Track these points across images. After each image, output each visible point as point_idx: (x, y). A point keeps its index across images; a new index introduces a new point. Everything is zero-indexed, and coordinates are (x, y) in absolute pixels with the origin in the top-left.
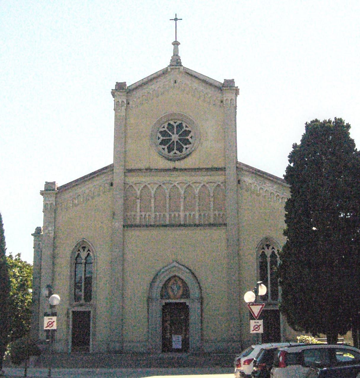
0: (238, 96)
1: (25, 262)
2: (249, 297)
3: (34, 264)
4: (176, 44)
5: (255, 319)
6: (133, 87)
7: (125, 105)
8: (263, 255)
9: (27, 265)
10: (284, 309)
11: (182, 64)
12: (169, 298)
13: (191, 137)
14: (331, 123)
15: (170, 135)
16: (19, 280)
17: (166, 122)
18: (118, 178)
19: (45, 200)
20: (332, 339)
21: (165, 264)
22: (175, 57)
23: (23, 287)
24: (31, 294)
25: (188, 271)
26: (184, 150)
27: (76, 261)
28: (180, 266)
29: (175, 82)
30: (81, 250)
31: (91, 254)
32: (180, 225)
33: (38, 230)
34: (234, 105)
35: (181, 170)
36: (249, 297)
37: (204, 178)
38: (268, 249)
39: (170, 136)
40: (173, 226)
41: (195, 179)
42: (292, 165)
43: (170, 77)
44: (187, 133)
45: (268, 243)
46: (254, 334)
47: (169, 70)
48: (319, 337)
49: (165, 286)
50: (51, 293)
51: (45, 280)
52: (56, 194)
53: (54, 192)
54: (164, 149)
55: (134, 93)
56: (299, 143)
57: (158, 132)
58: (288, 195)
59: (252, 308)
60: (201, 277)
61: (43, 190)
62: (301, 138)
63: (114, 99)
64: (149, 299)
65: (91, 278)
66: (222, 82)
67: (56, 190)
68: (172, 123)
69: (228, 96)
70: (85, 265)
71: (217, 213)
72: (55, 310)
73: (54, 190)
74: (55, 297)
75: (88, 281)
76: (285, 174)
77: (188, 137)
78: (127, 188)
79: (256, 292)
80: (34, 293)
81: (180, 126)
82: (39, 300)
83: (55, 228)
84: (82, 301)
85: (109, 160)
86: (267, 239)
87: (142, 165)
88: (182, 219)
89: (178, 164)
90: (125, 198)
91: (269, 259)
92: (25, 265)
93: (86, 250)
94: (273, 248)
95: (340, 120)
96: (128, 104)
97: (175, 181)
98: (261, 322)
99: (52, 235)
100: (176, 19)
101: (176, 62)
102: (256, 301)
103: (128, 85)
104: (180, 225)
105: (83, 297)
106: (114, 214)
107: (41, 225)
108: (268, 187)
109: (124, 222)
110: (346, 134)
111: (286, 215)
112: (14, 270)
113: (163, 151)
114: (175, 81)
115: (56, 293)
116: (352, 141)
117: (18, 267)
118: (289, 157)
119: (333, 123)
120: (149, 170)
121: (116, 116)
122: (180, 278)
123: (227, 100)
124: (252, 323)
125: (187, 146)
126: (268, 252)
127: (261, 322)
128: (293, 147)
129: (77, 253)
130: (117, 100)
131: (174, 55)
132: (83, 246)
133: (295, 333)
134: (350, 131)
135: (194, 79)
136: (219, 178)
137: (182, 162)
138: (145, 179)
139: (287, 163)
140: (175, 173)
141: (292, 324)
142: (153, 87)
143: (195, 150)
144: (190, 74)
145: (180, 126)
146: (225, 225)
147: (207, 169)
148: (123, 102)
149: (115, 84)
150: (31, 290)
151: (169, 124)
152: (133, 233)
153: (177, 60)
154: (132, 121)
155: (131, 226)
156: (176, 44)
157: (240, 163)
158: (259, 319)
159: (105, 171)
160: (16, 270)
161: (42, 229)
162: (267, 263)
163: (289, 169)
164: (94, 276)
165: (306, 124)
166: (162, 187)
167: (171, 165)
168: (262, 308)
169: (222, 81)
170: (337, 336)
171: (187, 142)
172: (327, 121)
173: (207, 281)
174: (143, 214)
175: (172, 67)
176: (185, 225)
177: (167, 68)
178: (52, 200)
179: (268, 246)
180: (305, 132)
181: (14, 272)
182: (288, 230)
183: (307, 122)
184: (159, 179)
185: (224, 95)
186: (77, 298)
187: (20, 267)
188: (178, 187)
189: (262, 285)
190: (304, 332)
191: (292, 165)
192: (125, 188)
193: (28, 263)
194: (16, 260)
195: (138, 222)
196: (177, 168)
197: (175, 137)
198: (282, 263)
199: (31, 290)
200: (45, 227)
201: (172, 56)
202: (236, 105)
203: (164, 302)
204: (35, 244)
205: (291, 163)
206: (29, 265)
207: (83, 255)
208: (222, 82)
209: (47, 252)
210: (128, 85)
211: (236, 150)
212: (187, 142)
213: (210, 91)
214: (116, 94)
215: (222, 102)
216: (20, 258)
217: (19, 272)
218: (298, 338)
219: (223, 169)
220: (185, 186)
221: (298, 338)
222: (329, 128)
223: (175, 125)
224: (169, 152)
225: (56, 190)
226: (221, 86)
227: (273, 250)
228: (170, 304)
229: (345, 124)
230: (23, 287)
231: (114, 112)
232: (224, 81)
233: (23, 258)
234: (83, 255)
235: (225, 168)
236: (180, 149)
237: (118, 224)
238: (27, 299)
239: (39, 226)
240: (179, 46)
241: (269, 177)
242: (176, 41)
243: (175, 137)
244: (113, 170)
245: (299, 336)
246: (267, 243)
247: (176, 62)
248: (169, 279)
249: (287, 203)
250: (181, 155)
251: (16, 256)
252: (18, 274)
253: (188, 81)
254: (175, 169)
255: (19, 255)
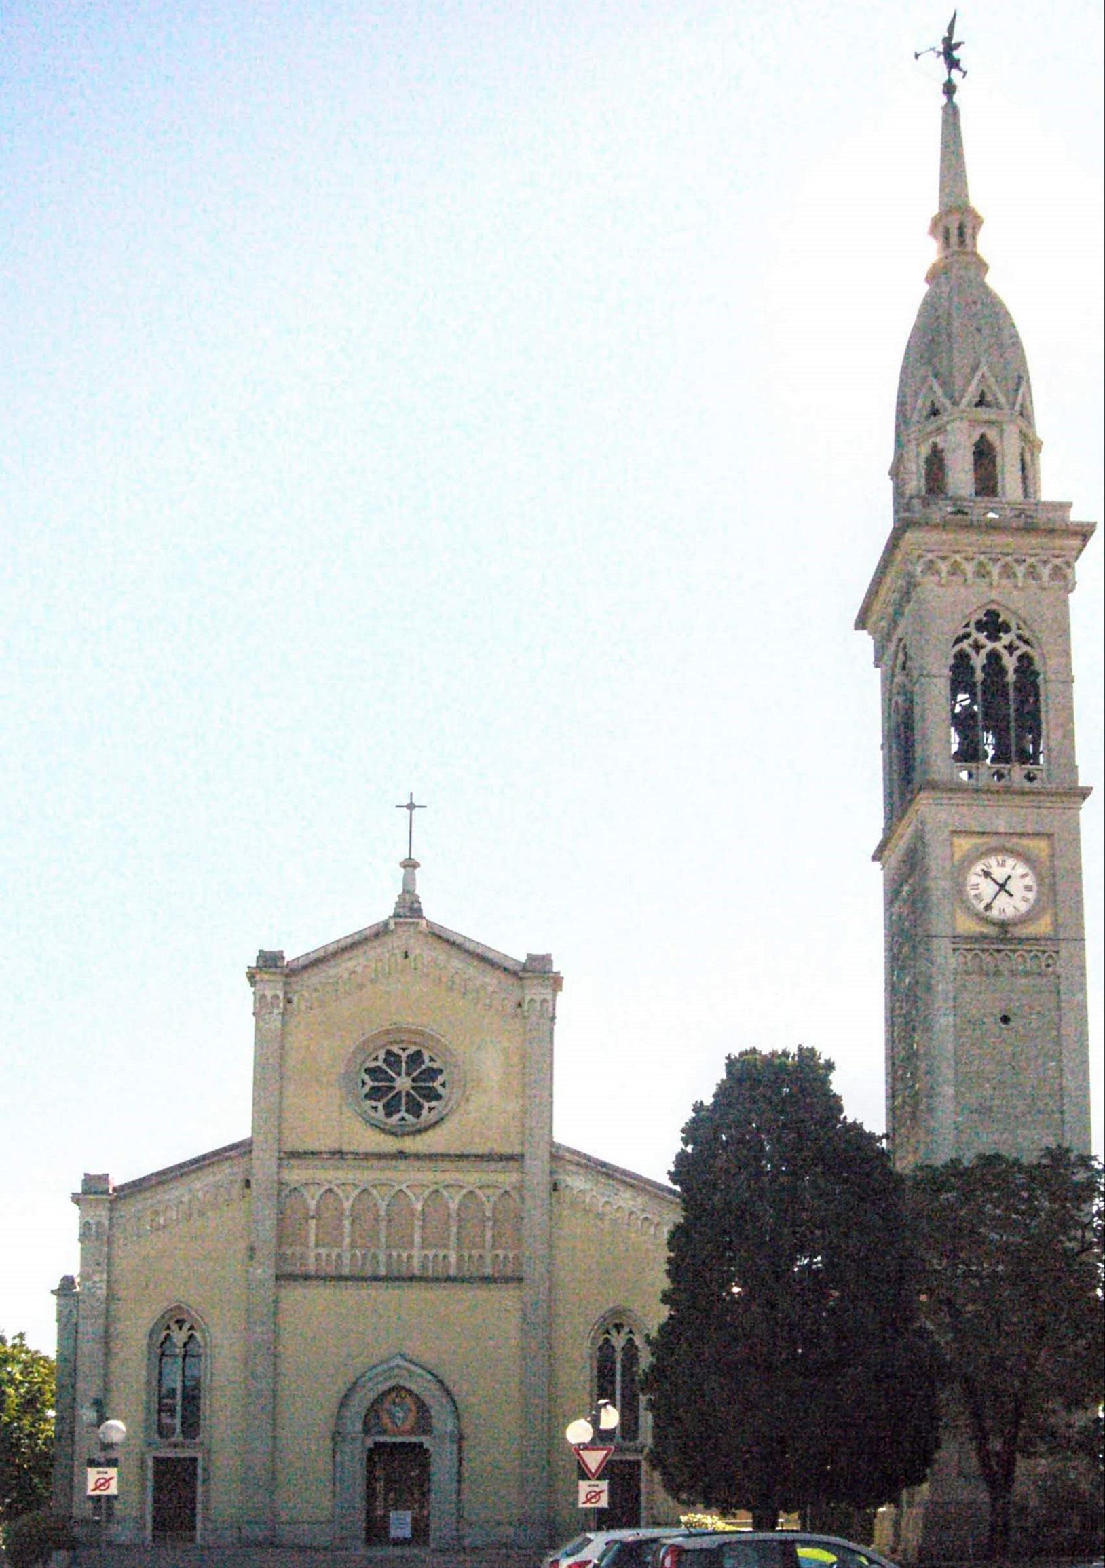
0: (559, 993)
1: (37, 1352)
2: (578, 1432)
3: (60, 1354)
4: (410, 865)
5: (589, 1479)
6: (302, 962)
7: (281, 1005)
8: (606, 1350)
9: (41, 1358)
10: (656, 1460)
11: (424, 914)
12: (383, 1432)
13: (443, 1085)
14: (788, 1057)
15: (392, 1077)
16: (22, 1390)
17: (383, 1047)
18: (264, 1165)
19: (82, 1217)
20: (765, 1522)
21: (375, 1361)
22: (407, 897)
23: (31, 1403)
24: (53, 1421)
25: (429, 1377)
26: (425, 1112)
27: (161, 1351)
28: (412, 1367)
29: (406, 956)
30: (174, 1327)
31: (198, 1335)
32: (412, 1278)
33: (68, 1282)
34: (551, 1015)
35: (417, 1156)
36: (578, 1432)
37: (472, 1177)
38: (619, 1332)
39: (392, 1079)
40: (397, 1279)
41: (449, 1177)
42: (689, 1149)
43: (396, 943)
44: (433, 1073)
45: (617, 1321)
46: (583, 1509)
47: (392, 926)
48: (734, 1516)
49: (374, 1408)
50: (102, 1419)
51: (88, 1388)
52: (111, 1202)
53: (104, 1197)
54: (375, 1108)
55: (306, 976)
56: (708, 1101)
57: (363, 1070)
58: (674, 1216)
59: (584, 1457)
60: (460, 1388)
61: (80, 1191)
62: (714, 1090)
63: (253, 989)
64: (337, 1436)
65: (197, 1387)
66: (523, 959)
67: (111, 1192)
68: (396, 1049)
69: (535, 992)
70: (184, 1359)
71: (500, 1252)
72: (113, 1455)
73: (106, 1192)
74: (112, 1426)
75: (192, 1397)
76: (673, 1169)
77: (436, 1084)
78: (284, 1192)
79: (595, 1421)
80: (60, 1419)
81: (416, 1058)
82: (72, 1432)
83: (109, 1277)
84: (178, 1438)
85: (238, 1128)
86: (617, 1312)
87: (325, 1143)
88: (416, 1263)
89: (410, 1144)
90: (280, 1216)
91: (619, 1357)
92: (36, 1359)
93: (186, 1326)
94: (631, 1332)
95: (812, 1051)
96: (289, 1001)
97: (401, 1183)
98: (604, 1485)
99: (102, 1292)
100: (411, 806)
101: (409, 908)
102: (593, 1440)
103: (289, 957)
104: (412, 1278)
105: (178, 1430)
106: (252, 1249)
107: (74, 1270)
108: (626, 1199)
109: (277, 1269)
110: (825, 1082)
111: (670, 1261)
112: (9, 1369)
113: (373, 1114)
114: (406, 953)
115: (117, 1418)
116: (837, 1099)
117: (19, 1362)
118: (683, 1131)
119: (793, 1058)
120: (339, 1154)
121: (258, 1030)
122: (410, 1392)
123: (532, 1000)
124: (584, 1487)
125: (433, 1104)
126: (619, 1341)
127: (604, 1485)
128: (693, 1110)
129: (165, 1333)
130: (261, 993)
131: (405, 891)
132: (177, 1317)
133: (680, 1507)
134: (833, 1077)
135: (454, 952)
136: (507, 1178)
137: (418, 1138)
138: (330, 1175)
139: (678, 1146)
140: (402, 1164)
141: (673, 1489)
142: (351, 964)
143: (451, 1112)
144: (440, 937)
145: (416, 1058)
146: (520, 1280)
147: (480, 1157)
148: (276, 997)
149: (83, 1177)
150: (51, 1413)
151: (389, 1053)
152: (294, 1295)
153: (412, 903)
154: (298, 1038)
155: (292, 1277)
156: (410, 865)
157: (559, 1146)
158: (599, 1479)
159: (232, 1153)
160: (15, 1370)
161: (77, 1280)
162: (614, 1363)
163: (681, 1158)
164: (205, 1383)
165: (728, 1058)
166: (370, 1194)
167: (390, 1144)
168: (607, 1455)
169: (523, 959)
170: (777, 1517)
171: (433, 1095)
172: (780, 1052)
173: (472, 1396)
174: (323, 1251)
175: (398, 920)
176: (423, 1279)
177: (386, 924)
178: (102, 1214)
179: (618, 1327)
180: (724, 1076)
181: (9, 1373)
182: (674, 1291)
183: (729, 1055)
184: (366, 1175)
185: (526, 991)
186: (164, 1432)
187: (25, 1363)
188: (409, 1193)
189: (609, 1407)
190: (700, 1506)
191: (689, 1149)
192: (280, 1191)
193: (44, 1353)
194: (14, 1346)
195: (312, 1269)
196: (407, 1151)
197: (403, 1083)
198: (655, 1360)
199: (51, 1413)
200: (85, 1276)
201: (400, 893)
202: (554, 1014)
203: (370, 1443)
204: (60, 1313)
205: (686, 1146)
206: (46, 1359)
207: (179, 1337)
208: (523, 959)
209: (90, 1329)
210: (289, 957)
211: (551, 1117)
212: (433, 1095)
213: (491, 979)
214: (258, 978)
215: (520, 1005)
216: (24, 1343)
217: (21, 1373)
218: (683, 1519)
219: (515, 1158)
220: (427, 1193)
221: (683, 1519)
222: (783, 1066)
223: (404, 1055)
224: (389, 1114)
225: (111, 1192)
226: (518, 968)
227: (631, 1335)
228: (384, 1445)
229: (822, 1061)
230: (31, 1403)
231: (254, 1019)
232: (526, 958)
233: (31, 1344)
234: (179, 1337)
235: (522, 1156)
236: (415, 1109)
237: (263, 1272)
238: (43, 1432)
239: (69, 1273)
240: (417, 871)
241: (628, 1180)
242: (410, 858)
243: (403, 1083)
244: (251, 1152)
245: (685, 1514)
246: (616, 1321)
247: (409, 908)
248: (385, 1394)
249: (673, 1234)
250: (417, 1123)
251: (14, 1338)
252: (18, 1377)
253: (440, 954)
254: (401, 1155)
255: (21, 1336)
